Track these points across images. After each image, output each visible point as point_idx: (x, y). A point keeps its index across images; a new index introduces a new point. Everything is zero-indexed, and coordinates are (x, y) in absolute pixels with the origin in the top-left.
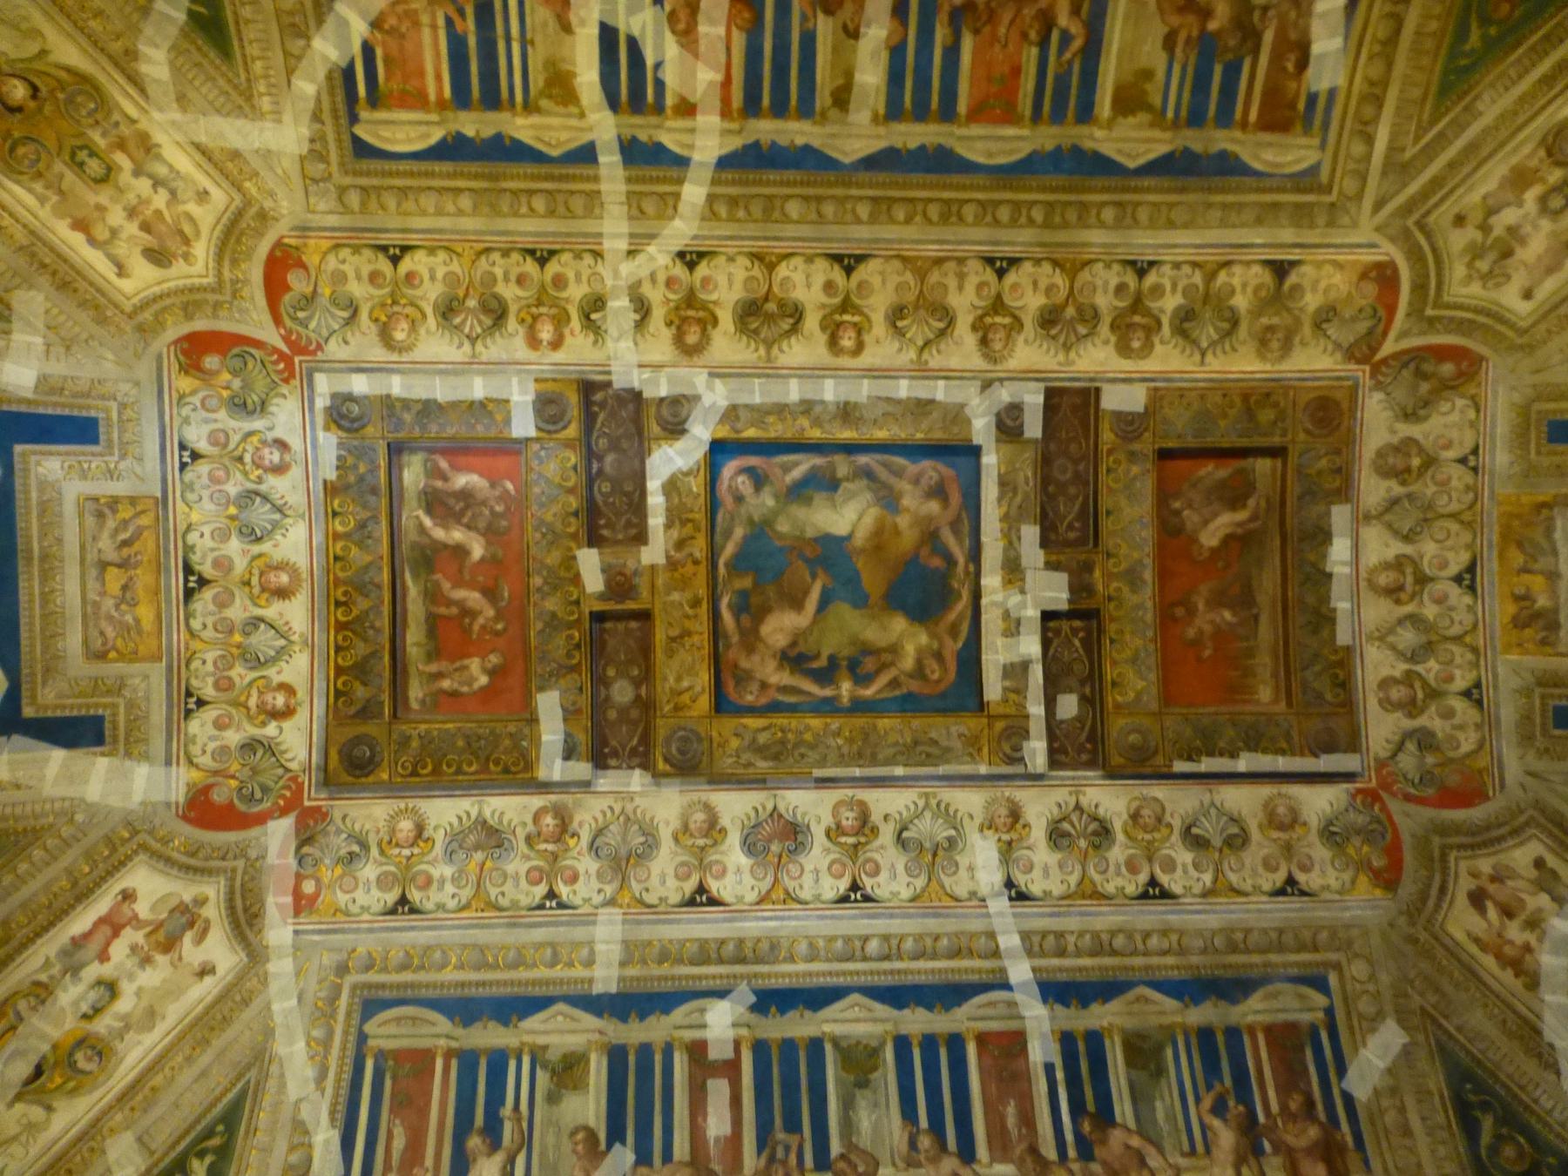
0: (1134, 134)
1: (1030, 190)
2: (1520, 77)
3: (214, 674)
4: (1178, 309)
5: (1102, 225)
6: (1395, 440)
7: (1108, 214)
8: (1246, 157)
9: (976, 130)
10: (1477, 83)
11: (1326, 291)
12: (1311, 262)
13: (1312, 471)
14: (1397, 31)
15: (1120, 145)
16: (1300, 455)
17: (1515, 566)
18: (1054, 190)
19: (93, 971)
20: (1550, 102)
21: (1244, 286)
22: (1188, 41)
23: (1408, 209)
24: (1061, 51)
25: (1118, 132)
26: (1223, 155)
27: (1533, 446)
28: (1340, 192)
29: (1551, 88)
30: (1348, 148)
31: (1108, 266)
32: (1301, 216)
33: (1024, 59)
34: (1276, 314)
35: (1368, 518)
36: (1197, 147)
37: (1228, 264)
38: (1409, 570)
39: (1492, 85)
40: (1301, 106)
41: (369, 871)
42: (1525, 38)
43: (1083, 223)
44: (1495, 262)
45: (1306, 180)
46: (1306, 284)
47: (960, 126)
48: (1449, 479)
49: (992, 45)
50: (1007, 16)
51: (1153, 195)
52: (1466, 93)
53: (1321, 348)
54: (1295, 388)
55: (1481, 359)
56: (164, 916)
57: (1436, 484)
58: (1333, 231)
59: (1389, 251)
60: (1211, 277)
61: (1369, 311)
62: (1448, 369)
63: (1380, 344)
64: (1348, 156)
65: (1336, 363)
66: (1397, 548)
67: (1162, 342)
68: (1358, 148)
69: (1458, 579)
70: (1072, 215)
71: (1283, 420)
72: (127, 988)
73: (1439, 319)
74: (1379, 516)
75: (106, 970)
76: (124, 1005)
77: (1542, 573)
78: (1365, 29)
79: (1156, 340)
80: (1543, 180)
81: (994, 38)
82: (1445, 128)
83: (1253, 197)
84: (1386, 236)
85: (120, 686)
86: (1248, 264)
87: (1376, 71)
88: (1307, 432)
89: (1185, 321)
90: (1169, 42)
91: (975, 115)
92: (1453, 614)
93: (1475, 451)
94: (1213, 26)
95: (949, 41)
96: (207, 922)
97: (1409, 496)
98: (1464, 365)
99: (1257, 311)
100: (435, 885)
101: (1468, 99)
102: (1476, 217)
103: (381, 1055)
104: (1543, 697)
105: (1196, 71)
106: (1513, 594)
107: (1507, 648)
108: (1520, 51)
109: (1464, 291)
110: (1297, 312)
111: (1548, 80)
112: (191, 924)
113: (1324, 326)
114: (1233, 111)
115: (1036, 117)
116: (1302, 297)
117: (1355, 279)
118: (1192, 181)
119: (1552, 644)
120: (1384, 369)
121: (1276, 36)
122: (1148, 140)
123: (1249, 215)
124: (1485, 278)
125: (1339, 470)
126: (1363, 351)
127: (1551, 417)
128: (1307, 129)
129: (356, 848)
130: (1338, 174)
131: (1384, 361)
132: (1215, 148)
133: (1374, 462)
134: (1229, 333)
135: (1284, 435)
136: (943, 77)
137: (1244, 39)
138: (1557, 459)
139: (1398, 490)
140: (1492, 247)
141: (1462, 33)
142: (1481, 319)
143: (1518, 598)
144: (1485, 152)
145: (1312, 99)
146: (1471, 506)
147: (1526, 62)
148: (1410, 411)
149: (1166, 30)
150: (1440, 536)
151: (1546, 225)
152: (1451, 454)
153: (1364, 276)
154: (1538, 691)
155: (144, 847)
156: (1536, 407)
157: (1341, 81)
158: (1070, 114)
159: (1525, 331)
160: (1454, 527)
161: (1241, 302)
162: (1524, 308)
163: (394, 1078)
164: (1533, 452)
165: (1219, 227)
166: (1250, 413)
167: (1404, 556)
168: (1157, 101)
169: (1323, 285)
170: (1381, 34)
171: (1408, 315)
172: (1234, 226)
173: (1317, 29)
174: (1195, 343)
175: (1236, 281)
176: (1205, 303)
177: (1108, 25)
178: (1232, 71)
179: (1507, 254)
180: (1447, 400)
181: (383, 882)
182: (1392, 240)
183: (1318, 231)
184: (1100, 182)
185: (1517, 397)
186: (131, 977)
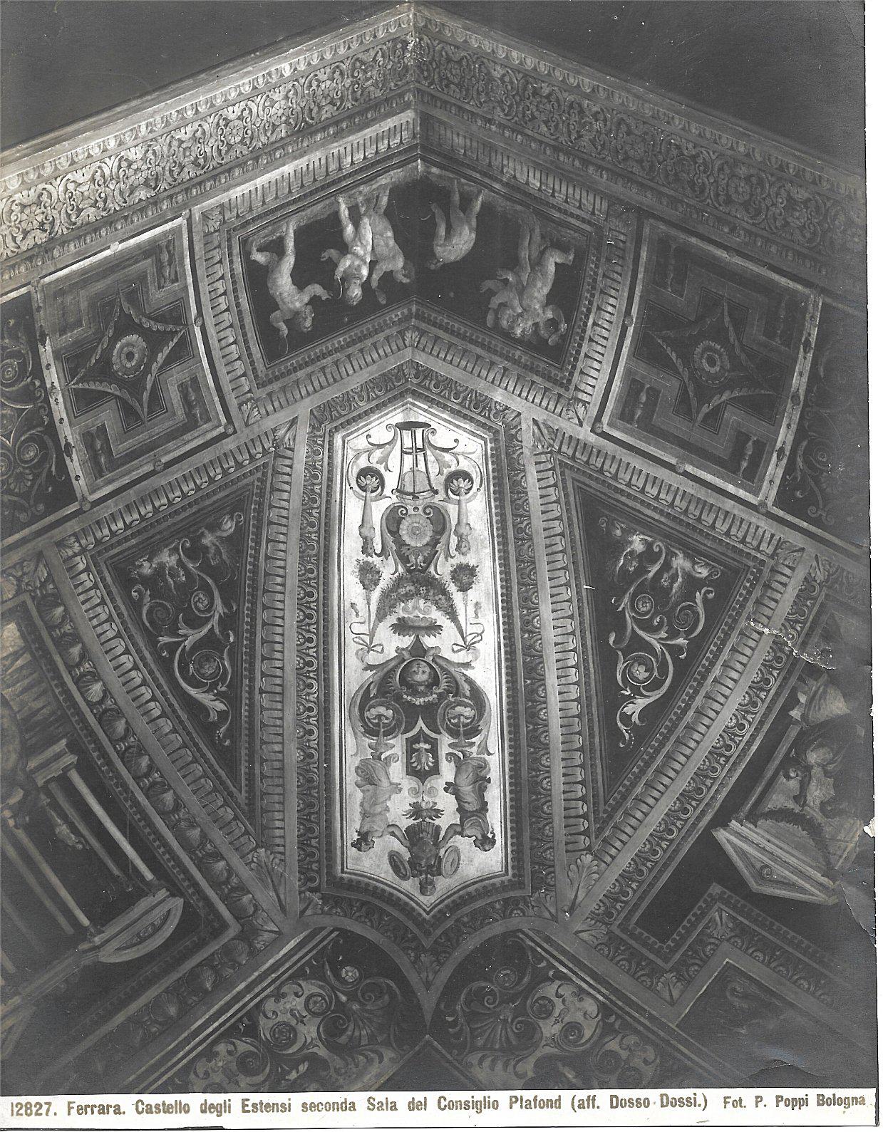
3: (627, 1061)
19: (448, 772)
41: (309, 1031)
56: (442, 852)
72: (408, 783)
75: (439, 783)
76: (397, 771)
85: (683, 974)
96: (404, 878)
100: (234, 1066)
103: (143, 889)
112: (414, 863)
129: (343, 1039)
155: (517, 883)
163: (115, 879)
181: (288, 1032)
186: (415, 792)
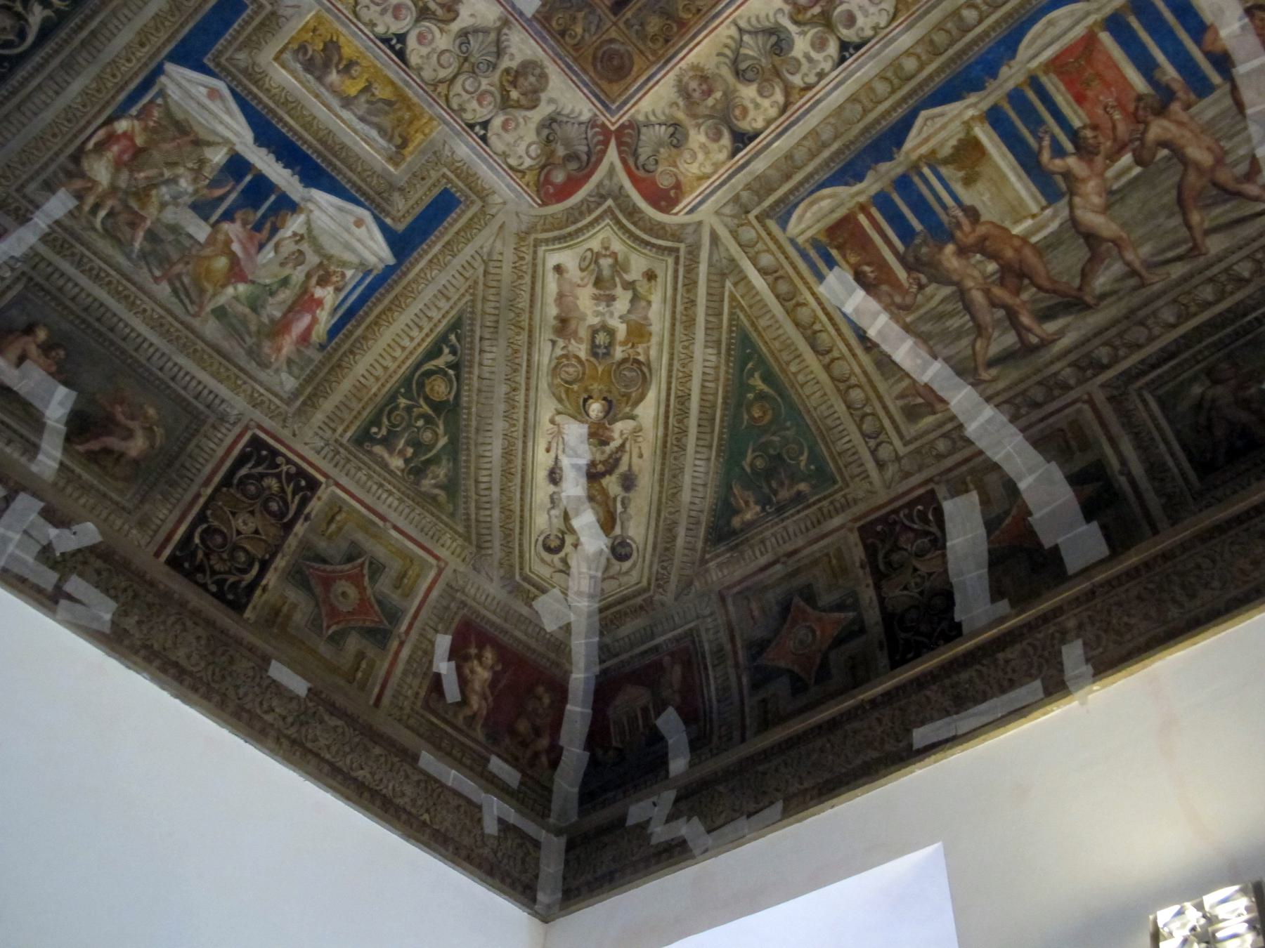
0: (943, 134)
1: (993, 28)
2: (703, 387)
4: (791, 45)
5: (908, 53)
6: (544, 96)
7: (910, 64)
8: (842, 191)
9: (1079, 31)
10: (727, 361)
11: (694, 156)
12: (724, 163)
13: (581, 15)
14: (813, 347)
15: (946, 119)
16: (600, 20)
17: (376, 85)
18: (975, 42)
20: (669, 389)
21: (757, 106)
22: (959, 225)
23: (693, 252)
24: (1055, 142)
25: (956, 126)
26: (860, 178)
27: (452, 176)
28: (750, 223)
29: (677, 397)
30: (773, 254)
31: (876, 28)
32: (762, 187)
33: (1080, 111)
34: (714, 106)
35: (506, 22)
36: (884, 167)
37: (784, 110)
38: (440, 12)
39: (717, 368)
40: (834, 252)
42: (724, 409)
43: (927, 40)
44: (600, 271)
45: (783, 213)
46: (713, 146)
47: (1095, 23)
48: (480, 104)
49: (1117, 99)
50: (1122, 128)
51: (886, 107)
52: (729, 350)
53: (658, 112)
54: (653, 63)
55: (544, 204)
57: (486, 92)
58: (730, 196)
59: (676, 218)
60: (788, 90)
61: (651, 168)
62: (559, 177)
63: (620, 152)
64: (768, 251)
65: (638, 111)
66: (464, 19)
67: (780, 10)
68: (766, 260)
69: (402, 38)
70: (940, 38)
71: (637, 32)
73: (599, 204)
74: (499, 31)
77: (356, 97)
78: (838, 330)
79: (787, 8)
80: (624, 343)
81: (1120, 106)
82: (721, 321)
83: (810, 168)
84: (689, 224)
86: (769, 122)
87: (804, 314)
88: (612, 41)
89: (778, 42)
90: (973, 214)
91: (1089, 42)
92: (378, 9)
93: (484, 139)
94: (950, 249)
95: (1157, 74)
97: (495, 66)
98: (551, 190)
99: (729, 95)
101: (724, 346)
102: (642, 287)
104: (261, 6)
105: (934, 213)
106: (357, 63)
107: (317, 16)
108: (720, 401)
109: (601, 236)
110: (701, 121)
111: (684, 399)
113: (671, 130)
114: (880, 209)
115: (1034, 82)
116: (707, 134)
117: (681, 178)
118: (865, 141)
119: (296, 52)
120: (601, 138)
121: (897, 279)
122: (927, 140)
123: (800, 155)
124: (596, 257)
125: (563, 33)
126: (627, 137)
127: (462, 206)
128: (814, 242)
130: (764, 234)
131: (606, 143)
132: (870, 177)
133: (542, 67)
134: (735, 62)
135: (627, 22)
136: (1143, 47)
137: (917, 259)
138: (429, 182)
139: (506, 63)
140: (613, 278)
141: (768, 378)
142: (572, 228)
143: (351, 64)
144: (679, 328)
145: (831, 263)
146: (447, 101)
147: (711, 397)
148: (555, 126)
149: (983, 219)
150: (444, 59)
151: (594, 321)
152: (497, 122)
153: (678, 186)
154: (269, 8)
156: (479, 204)
157: (821, 289)
158: (1007, 107)
159: (537, 243)
160: (443, 74)
161: (748, 92)
162: (553, 259)
164: (448, 173)
165: (813, 129)
166: (667, 14)
167: (454, 19)
168: (944, 171)
169: (701, 156)
170: (824, 336)
171: (621, 187)
172: (805, 138)
173: (873, 304)
174: (754, 33)
175: (766, 103)
176: (774, 66)
177: (1034, 188)
178: (906, 233)
179: (598, 282)
180: (538, 156)
182: (683, 226)
183: (741, 187)
184: (938, 81)
185: (497, 199)
